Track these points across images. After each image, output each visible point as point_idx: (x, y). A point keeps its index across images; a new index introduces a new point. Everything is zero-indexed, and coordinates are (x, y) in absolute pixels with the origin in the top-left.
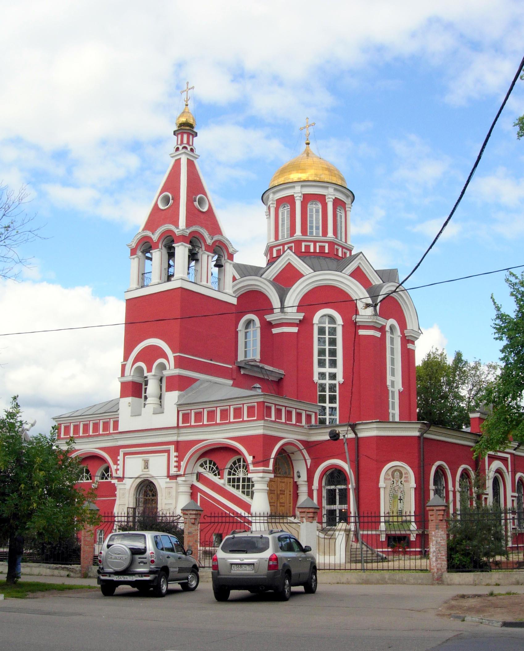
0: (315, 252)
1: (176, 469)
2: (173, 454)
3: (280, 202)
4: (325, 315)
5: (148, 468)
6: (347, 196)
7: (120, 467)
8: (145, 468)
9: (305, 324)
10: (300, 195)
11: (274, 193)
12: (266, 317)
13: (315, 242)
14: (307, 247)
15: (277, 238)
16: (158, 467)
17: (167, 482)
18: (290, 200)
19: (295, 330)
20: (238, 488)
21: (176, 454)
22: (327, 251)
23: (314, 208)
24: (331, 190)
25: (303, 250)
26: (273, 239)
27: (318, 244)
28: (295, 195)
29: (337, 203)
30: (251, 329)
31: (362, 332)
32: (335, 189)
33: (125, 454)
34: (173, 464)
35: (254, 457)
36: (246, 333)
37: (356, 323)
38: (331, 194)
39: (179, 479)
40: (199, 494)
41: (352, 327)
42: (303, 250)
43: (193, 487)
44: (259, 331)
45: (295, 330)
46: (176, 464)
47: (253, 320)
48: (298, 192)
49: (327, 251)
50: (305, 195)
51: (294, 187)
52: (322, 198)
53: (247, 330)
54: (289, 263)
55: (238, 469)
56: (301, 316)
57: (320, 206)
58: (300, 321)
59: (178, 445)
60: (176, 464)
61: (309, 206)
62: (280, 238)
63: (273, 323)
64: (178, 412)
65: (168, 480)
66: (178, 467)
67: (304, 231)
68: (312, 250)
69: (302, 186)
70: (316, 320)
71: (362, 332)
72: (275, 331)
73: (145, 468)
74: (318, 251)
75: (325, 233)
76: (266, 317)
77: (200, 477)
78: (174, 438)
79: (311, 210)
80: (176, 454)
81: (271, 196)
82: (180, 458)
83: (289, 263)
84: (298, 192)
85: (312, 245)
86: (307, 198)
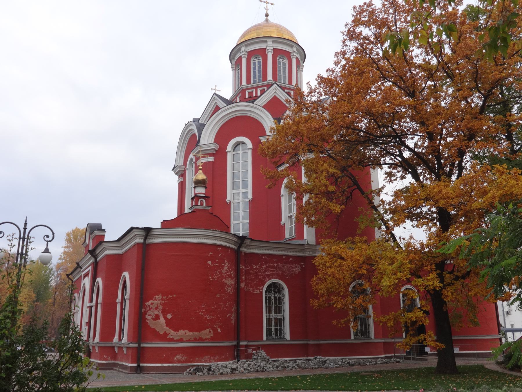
3: (251, 54)
10: (272, 48)
11: (246, 46)
12: (260, 138)
15: (248, 82)
18: (263, 52)
23: (283, 62)
24: (295, 49)
26: (244, 82)
28: (268, 48)
30: (240, 151)
32: (297, 50)
36: (234, 154)
44: (250, 152)
47: (243, 143)
48: (270, 46)
50: (275, 50)
51: (266, 42)
52: (287, 55)
53: (234, 153)
54: (275, 96)
62: (252, 82)
69: (273, 42)
75: (290, 82)
76: (260, 138)
81: (243, 49)
83: (275, 96)
84: (270, 46)
86: (277, 52)
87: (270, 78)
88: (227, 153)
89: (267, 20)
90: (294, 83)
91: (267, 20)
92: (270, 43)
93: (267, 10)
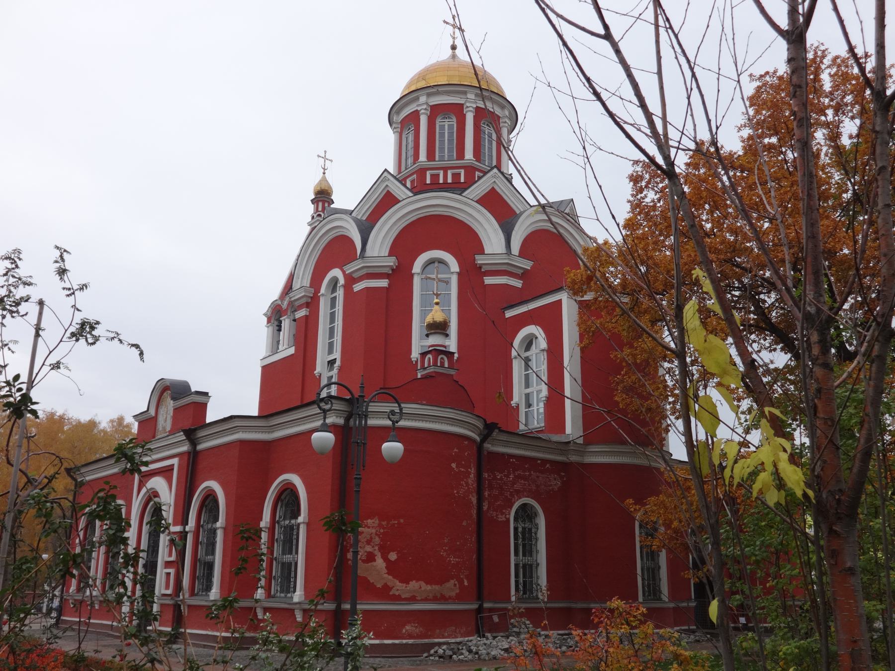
0: (445, 182)
3: (404, 123)
4: (431, 262)
6: (503, 107)
9: (400, 276)
11: (398, 113)
13: (445, 169)
14: (435, 177)
18: (415, 115)
19: (384, 283)
22: (462, 180)
23: (447, 124)
24: (471, 96)
25: (428, 181)
27: (450, 173)
29: (480, 114)
31: (489, 280)
37: (480, 268)
38: (471, 102)
41: (471, 275)
42: (428, 181)
45: (384, 283)
48: (423, 104)
49: (462, 180)
51: (417, 99)
52: (457, 110)
56: (392, 262)
57: (455, 119)
58: (393, 270)
61: (439, 122)
63: (355, 275)
67: (431, 155)
68: (441, 181)
69: (429, 95)
70: (417, 267)
71: (489, 280)
72: (358, 287)
74: (450, 180)
75: (461, 154)
79: (442, 127)
85: (441, 173)
86: (436, 111)
87: (423, 157)
88: (319, 297)
89: (454, 56)
90: (469, 154)
91: (454, 56)
92: (423, 99)
93: (454, 38)
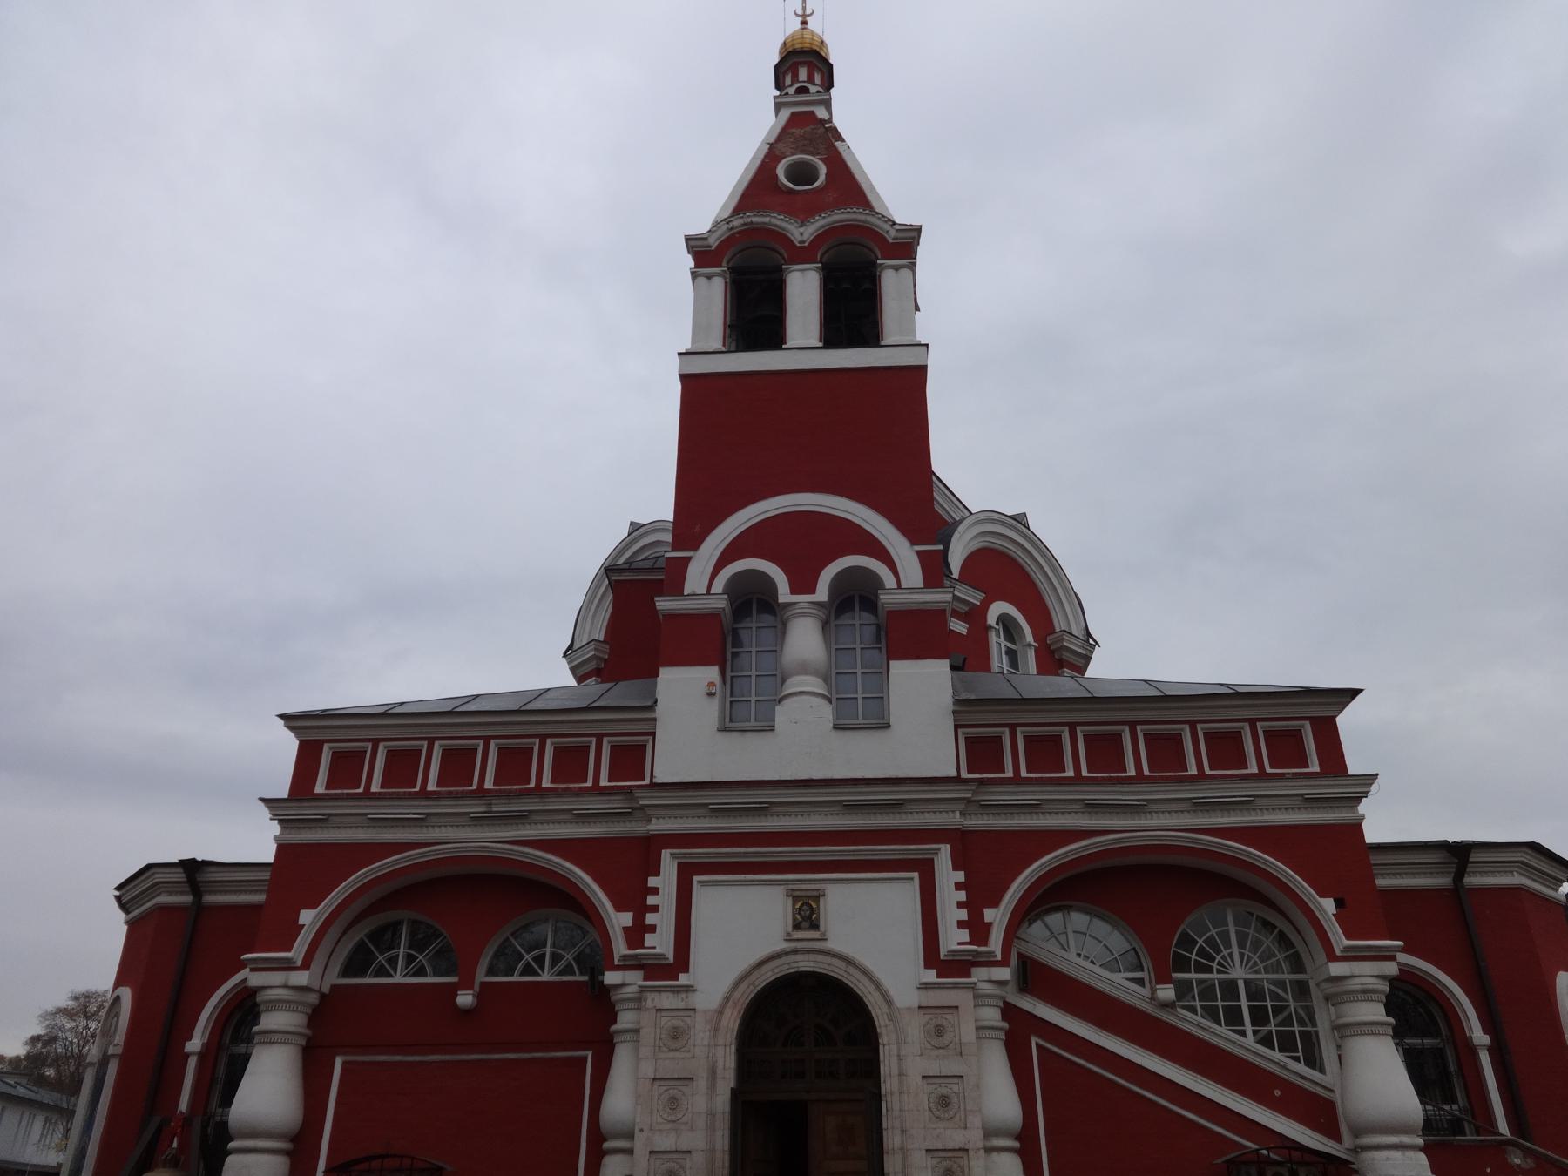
1: (964, 935)
2: (948, 876)
5: (815, 926)
7: (664, 920)
8: (797, 927)
16: (875, 931)
17: (926, 986)
20: (1234, 1017)
21: (960, 876)
33: (686, 873)
34: (951, 912)
35: (1339, 903)
39: (979, 974)
40: (1034, 1040)
43: (1009, 1011)
46: (963, 915)
55: (1218, 951)
59: (966, 846)
60: (963, 915)
64: (957, 727)
65: (931, 976)
66: (977, 929)
73: (797, 927)
77: (1034, 976)
78: (954, 819)
80: (960, 876)
82: (979, 895)
